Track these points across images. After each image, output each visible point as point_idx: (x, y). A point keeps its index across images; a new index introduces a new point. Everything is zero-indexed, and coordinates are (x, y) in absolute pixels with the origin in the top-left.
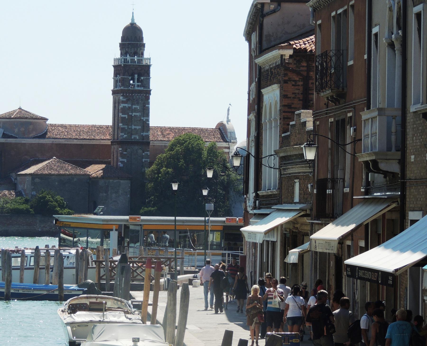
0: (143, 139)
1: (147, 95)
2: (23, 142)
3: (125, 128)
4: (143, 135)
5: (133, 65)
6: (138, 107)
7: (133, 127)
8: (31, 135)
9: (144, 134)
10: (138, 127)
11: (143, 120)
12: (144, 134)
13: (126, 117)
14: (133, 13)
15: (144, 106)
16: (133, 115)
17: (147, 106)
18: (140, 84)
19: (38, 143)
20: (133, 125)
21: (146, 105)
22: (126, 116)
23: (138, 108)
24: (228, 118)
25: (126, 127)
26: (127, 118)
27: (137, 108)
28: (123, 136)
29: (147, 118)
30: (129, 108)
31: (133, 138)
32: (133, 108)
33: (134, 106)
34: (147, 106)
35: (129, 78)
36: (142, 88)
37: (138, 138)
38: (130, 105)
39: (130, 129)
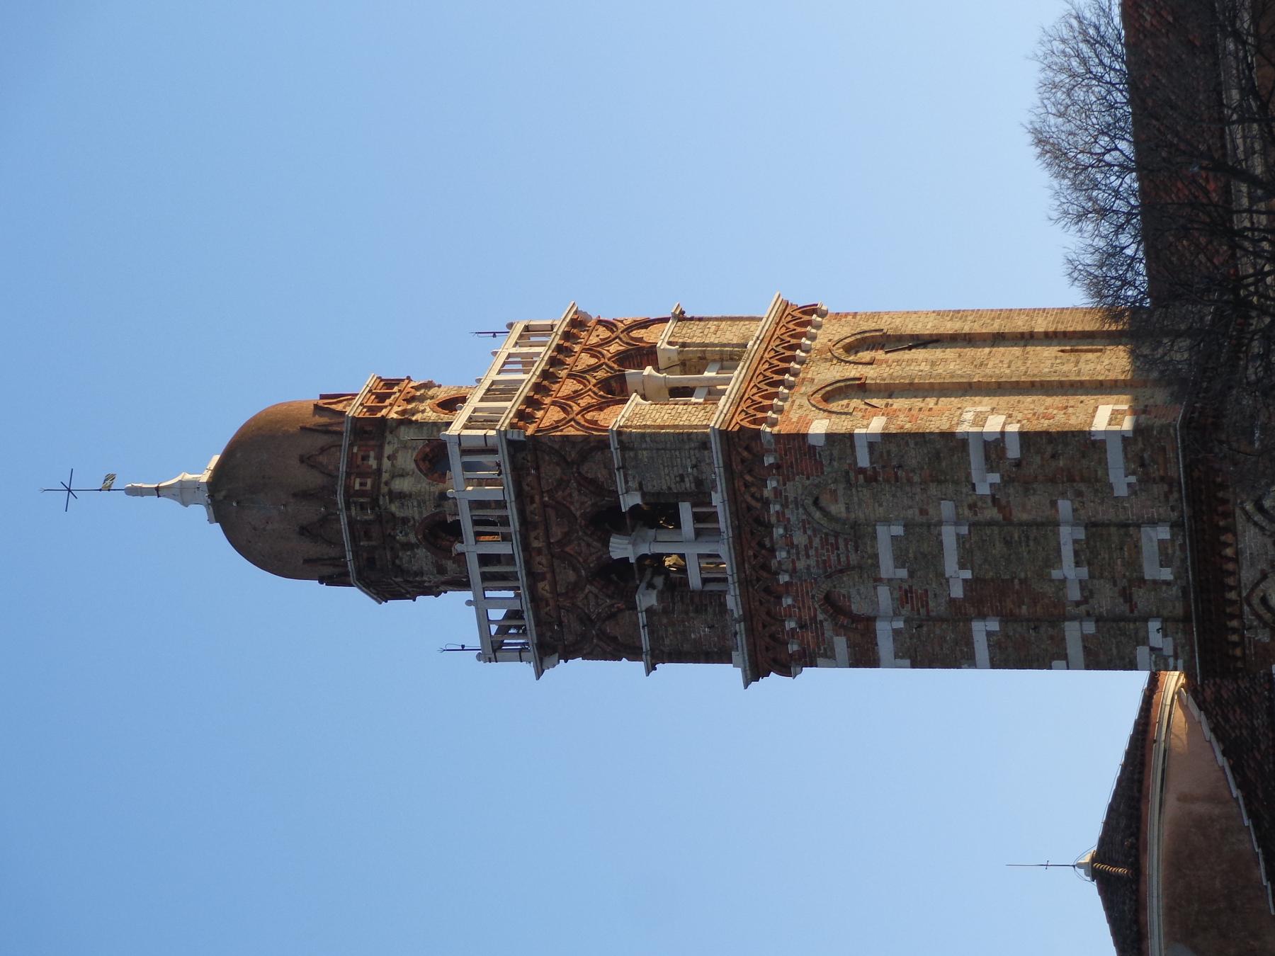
0: (1171, 482)
3: (1085, 638)
4: (1129, 485)
6: (886, 536)
7: (1069, 570)
9: (1120, 480)
10: (1068, 536)
11: (991, 485)
12: (1120, 480)
13: (989, 634)
14: (134, 492)
15: (871, 478)
16: (968, 574)
17: (863, 460)
20: (1056, 574)
21: (862, 471)
22: (981, 630)
23: (898, 530)
25: (1073, 633)
26: (994, 625)
27: (894, 538)
28: (1152, 649)
29: (976, 457)
30: (905, 596)
31: (1167, 574)
32: (903, 573)
33: (887, 567)
34: (863, 460)
35: (649, 611)
36: (717, 499)
37: (1164, 533)
38: (884, 596)
39: (1088, 593)
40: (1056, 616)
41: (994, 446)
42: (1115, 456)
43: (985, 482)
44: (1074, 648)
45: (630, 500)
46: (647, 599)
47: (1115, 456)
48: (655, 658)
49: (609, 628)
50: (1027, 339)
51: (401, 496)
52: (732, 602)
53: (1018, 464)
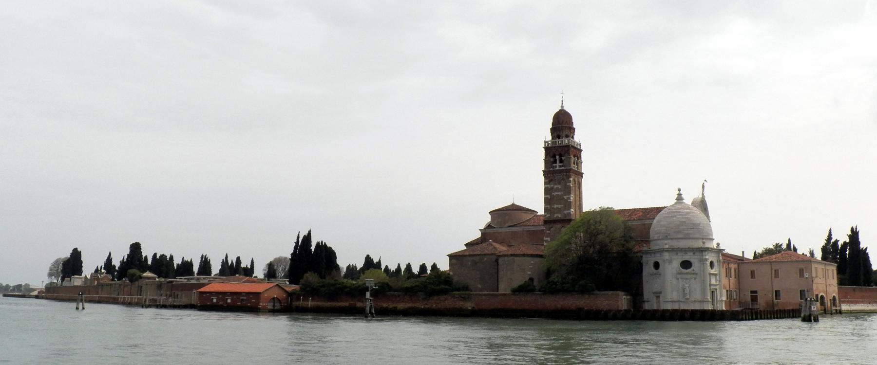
1: (568, 174)
2: (500, 231)
5: (554, 147)
7: (555, 206)
8: (507, 225)
9: (566, 212)
12: (566, 212)
15: (566, 185)
17: (568, 184)
18: (562, 164)
19: (512, 232)
22: (549, 196)
24: (703, 194)
26: (549, 198)
30: (552, 188)
33: (556, 186)
34: (568, 184)
36: (563, 168)
38: (552, 186)
39: (553, 208)
40: (550, 204)
41: (569, 198)
42: (568, 211)
43: (565, 197)
44: (547, 206)
45: (563, 158)
46: (552, 159)
47: (568, 211)
48: (545, 160)
49: (548, 155)
50: (580, 201)
51: (563, 133)
52: (551, 169)
53: (567, 201)
